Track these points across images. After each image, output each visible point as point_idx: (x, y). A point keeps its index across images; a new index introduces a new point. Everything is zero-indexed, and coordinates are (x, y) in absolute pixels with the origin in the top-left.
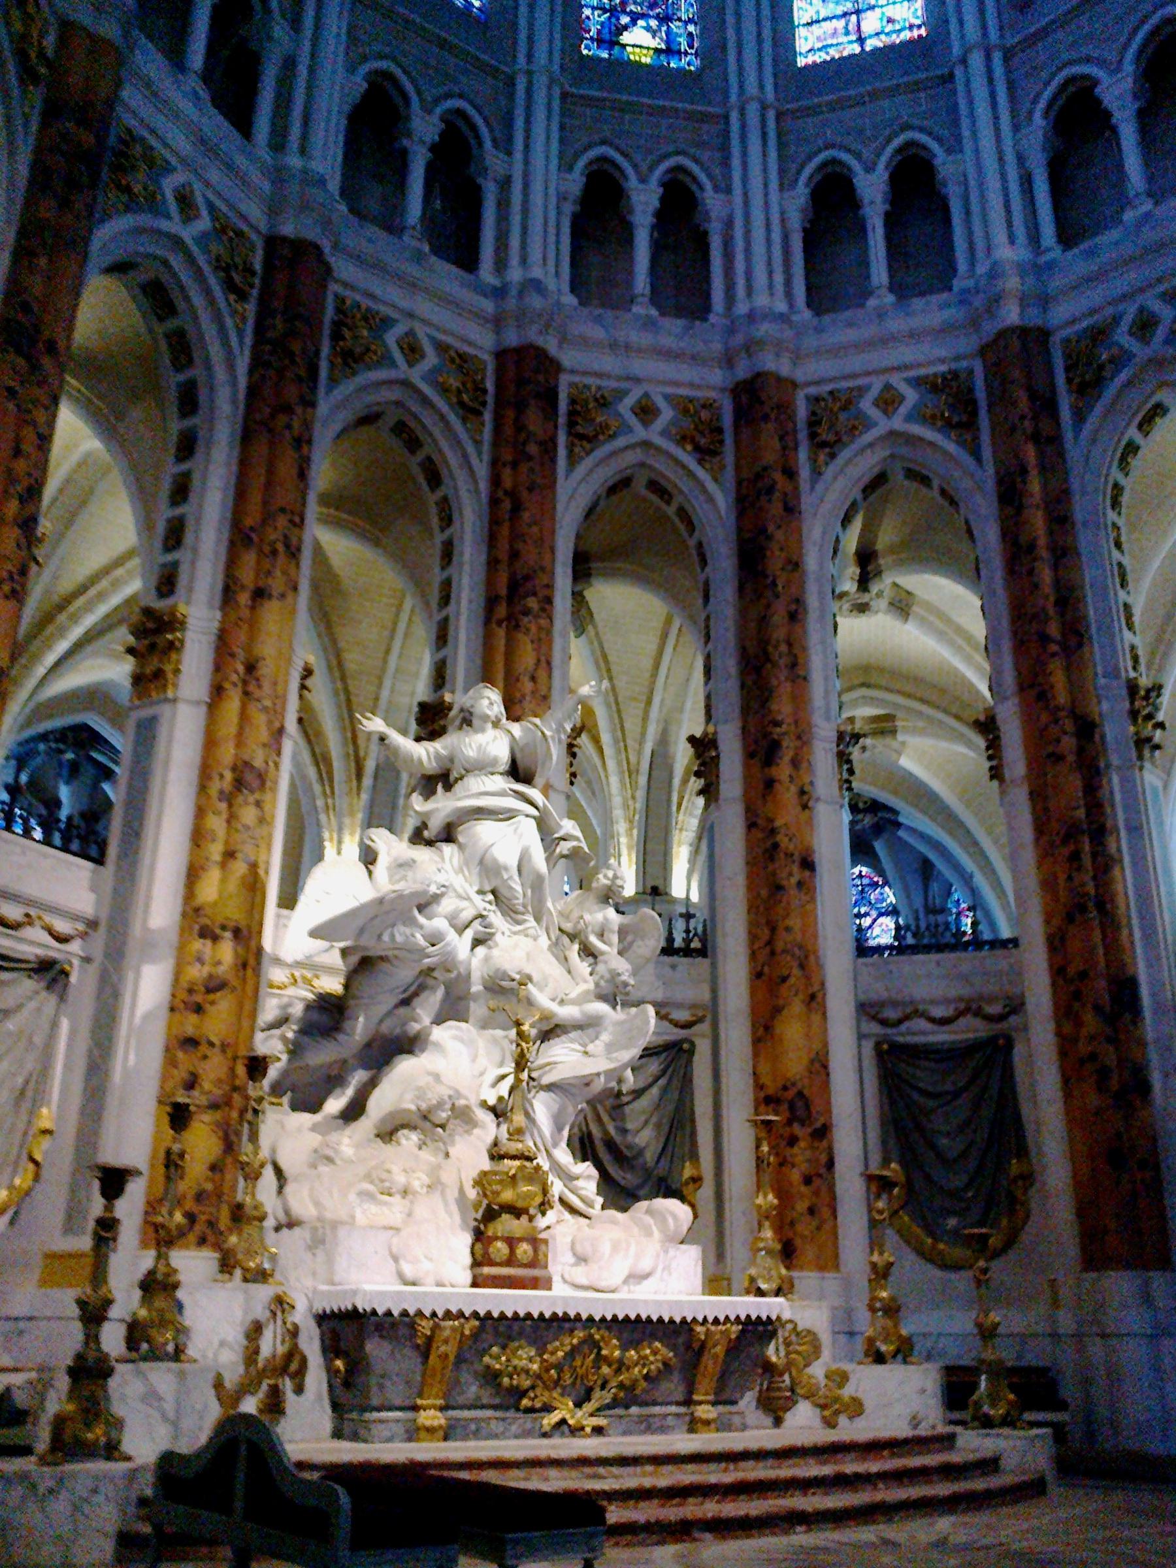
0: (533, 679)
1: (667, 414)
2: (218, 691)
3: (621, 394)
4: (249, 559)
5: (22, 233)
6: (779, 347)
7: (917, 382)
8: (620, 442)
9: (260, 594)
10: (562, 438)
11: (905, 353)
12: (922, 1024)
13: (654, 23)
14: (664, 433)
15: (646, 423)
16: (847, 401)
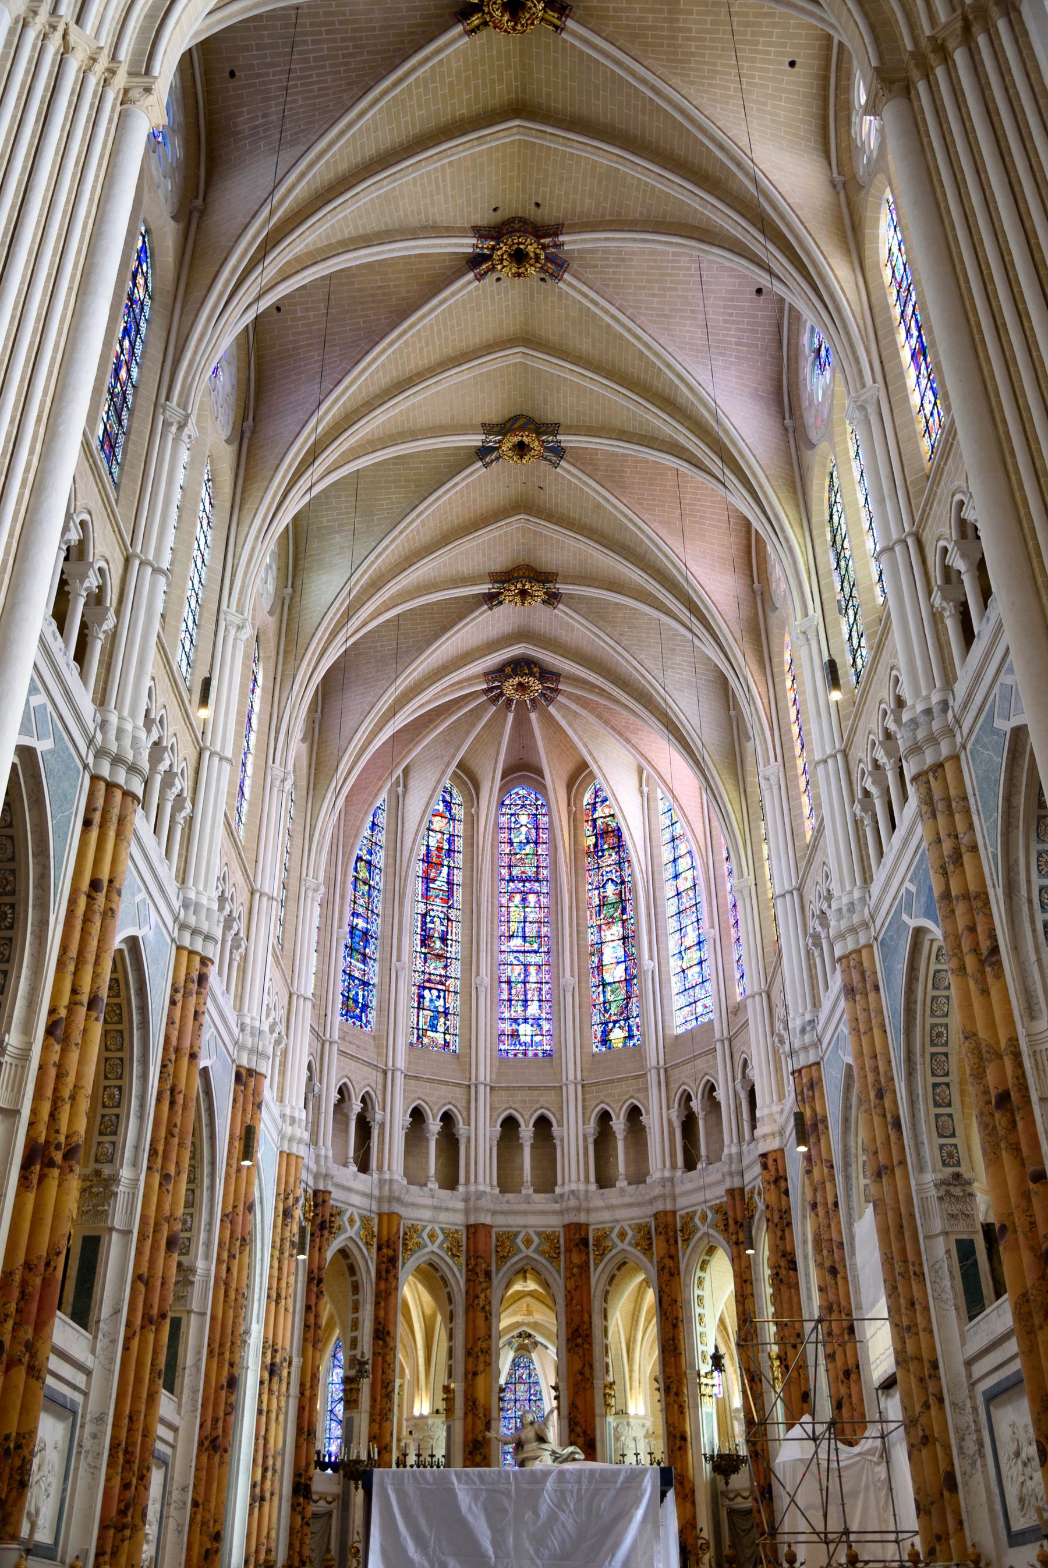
0: (582, 1373)
1: (630, 1233)
2: (466, 1414)
3: (612, 1229)
4: (471, 1359)
5: (377, 1296)
6: (664, 1197)
7: (711, 1208)
8: (614, 1252)
9: (475, 1374)
10: (592, 1257)
11: (709, 1194)
12: (739, 1499)
14: (630, 1244)
15: (622, 1241)
16: (691, 1216)
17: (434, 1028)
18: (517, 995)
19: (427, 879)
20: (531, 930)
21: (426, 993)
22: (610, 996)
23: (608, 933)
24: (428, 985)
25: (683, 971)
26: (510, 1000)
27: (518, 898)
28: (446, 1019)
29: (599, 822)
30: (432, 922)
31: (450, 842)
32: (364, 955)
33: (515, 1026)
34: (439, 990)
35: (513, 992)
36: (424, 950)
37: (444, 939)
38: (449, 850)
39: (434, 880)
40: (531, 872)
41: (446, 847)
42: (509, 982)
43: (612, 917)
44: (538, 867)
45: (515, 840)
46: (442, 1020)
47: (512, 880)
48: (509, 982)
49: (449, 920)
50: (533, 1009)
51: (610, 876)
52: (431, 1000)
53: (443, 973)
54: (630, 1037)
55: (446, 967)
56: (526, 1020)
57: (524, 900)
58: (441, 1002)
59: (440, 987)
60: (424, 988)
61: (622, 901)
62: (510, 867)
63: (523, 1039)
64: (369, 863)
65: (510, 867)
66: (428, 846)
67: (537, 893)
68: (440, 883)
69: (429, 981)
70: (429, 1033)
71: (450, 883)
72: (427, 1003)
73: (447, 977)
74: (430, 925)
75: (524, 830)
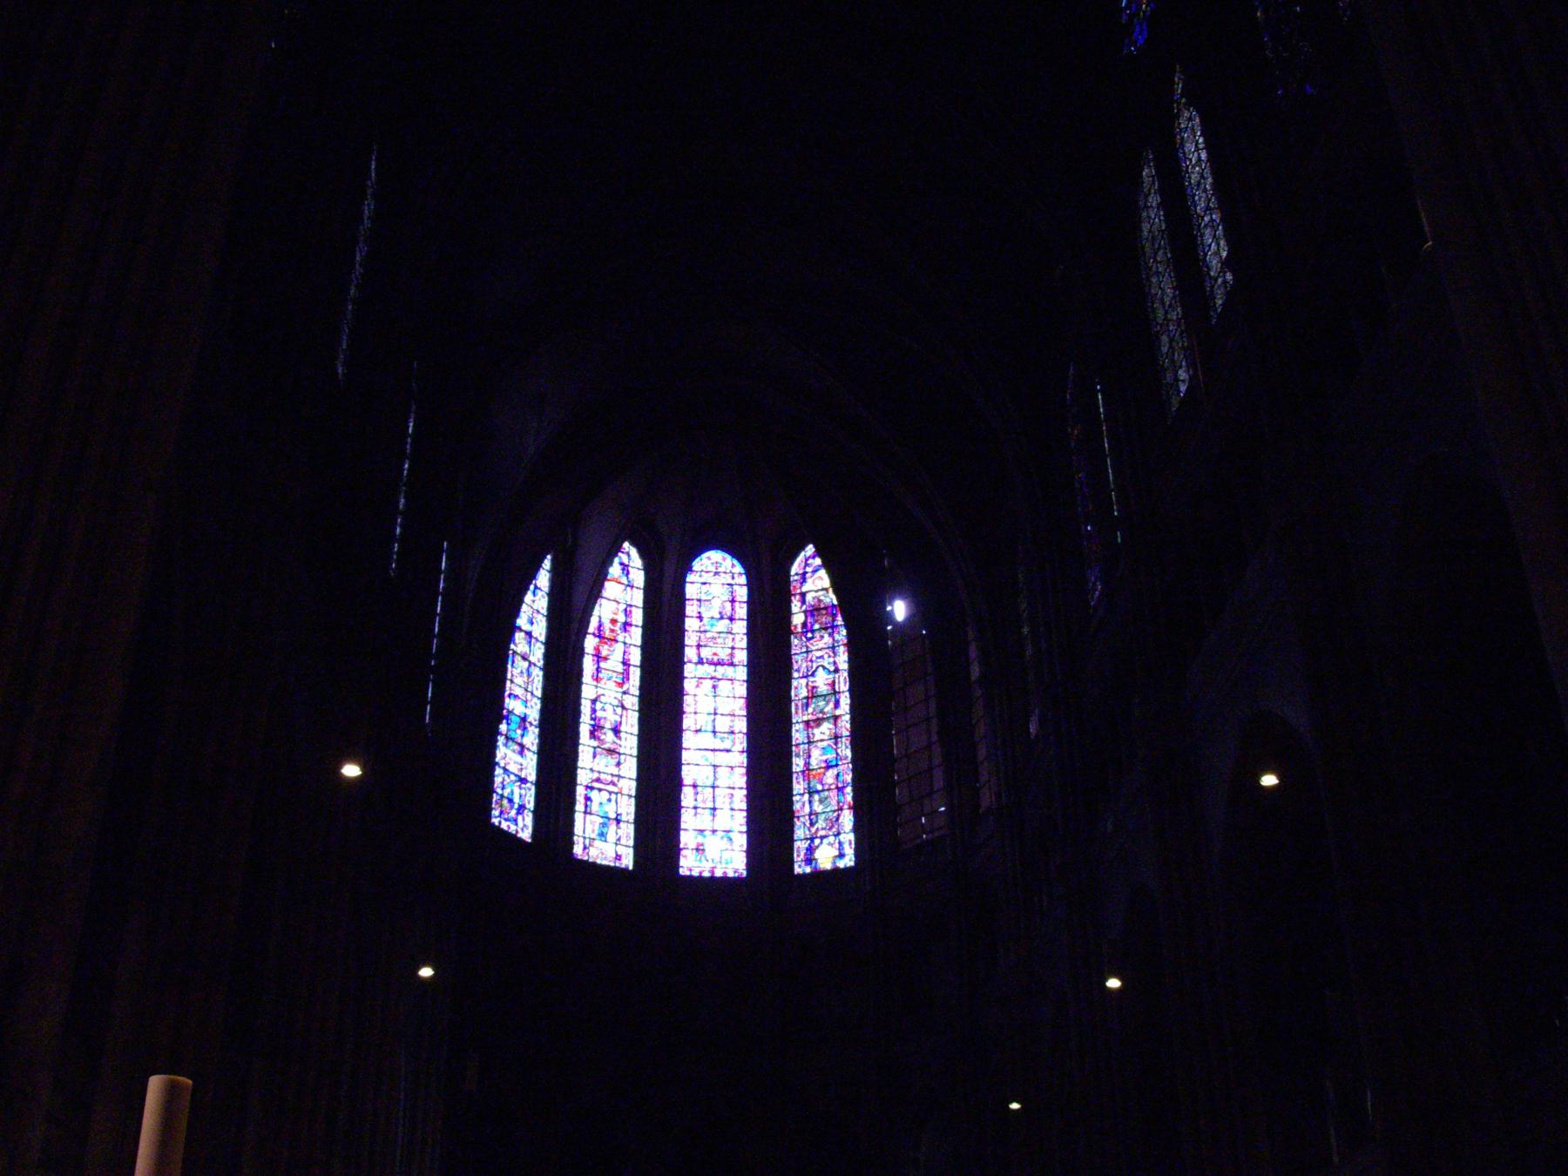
13: (831, 839)
17: (602, 835)
19: (598, 657)
20: (723, 724)
21: (594, 794)
22: (818, 807)
23: (817, 731)
24: (596, 785)
27: (708, 684)
29: (809, 598)
30: (603, 709)
31: (627, 613)
32: (522, 746)
33: (700, 839)
35: (700, 797)
37: (616, 731)
39: (606, 659)
40: (724, 654)
41: (621, 618)
42: (695, 786)
43: (822, 712)
46: (613, 827)
47: (701, 662)
48: (695, 786)
49: (623, 707)
51: (821, 662)
53: (615, 771)
54: (841, 856)
55: (618, 764)
57: (714, 687)
59: (611, 788)
60: (592, 788)
61: (835, 693)
62: (699, 646)
64: (529, 634)
68: (614, 663)
69: (598, 780)
71: (626, 663)
72: (595, 807)
74: (599, 714)
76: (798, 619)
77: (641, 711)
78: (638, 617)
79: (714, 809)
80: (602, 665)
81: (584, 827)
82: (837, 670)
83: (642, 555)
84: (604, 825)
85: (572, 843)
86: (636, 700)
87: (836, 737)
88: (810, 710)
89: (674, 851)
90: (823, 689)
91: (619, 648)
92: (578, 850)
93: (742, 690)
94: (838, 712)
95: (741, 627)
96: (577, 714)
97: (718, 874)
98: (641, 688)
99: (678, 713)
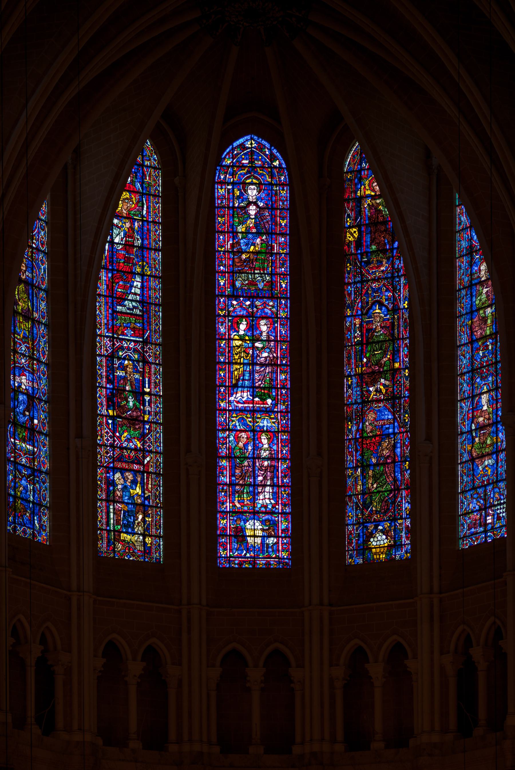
18: (243, 477)
25: (472, 460)
26: (232, 484)
28: (145, 515)
30: (123, 368)
31: (144, 234)
34: (135, 472)
36: (111, 412)
37: (139, 395)
38: (142, 248)
39: (121, 299)
43: (378, 363)
44: (271, 275)
45: (241, 229)
48: (230, 457)
49: (145, 362)
50: (265, 498)
52: (125, 488)
56: (255, 514)
57: (252, 327)
58: (138, 490)
59: (136, 467)
60: (115, 470)
61: (394, 339)
62: (232, 273)
63: (250, 540)
65: (232, 273)
66: (112, 243)
67: (272, 319)
69: (120, 459)
70: (123, 536)
73: (144, 452)
75: (252, 210)
76: (352, 235)
77: (164, 364)
78: (156, 234)
79: (255, 486)
80: (119, 308)
81: (109, 516)
82: (396, 309)
83: (158, 148)
84: (128, 513)
85: (96, 540)
86: (159, 350)
87: (392, 398)
88: (365, 360)
89: (212, 537)
90: (380, 334)
91: (137, 283)
92: (102, 545)
93: (283, 331)
94: (397, 365)
95: (281, 245)
96: (94, 375)
97: (261, 563)
98: (165, 334)
99: (210, 364)
